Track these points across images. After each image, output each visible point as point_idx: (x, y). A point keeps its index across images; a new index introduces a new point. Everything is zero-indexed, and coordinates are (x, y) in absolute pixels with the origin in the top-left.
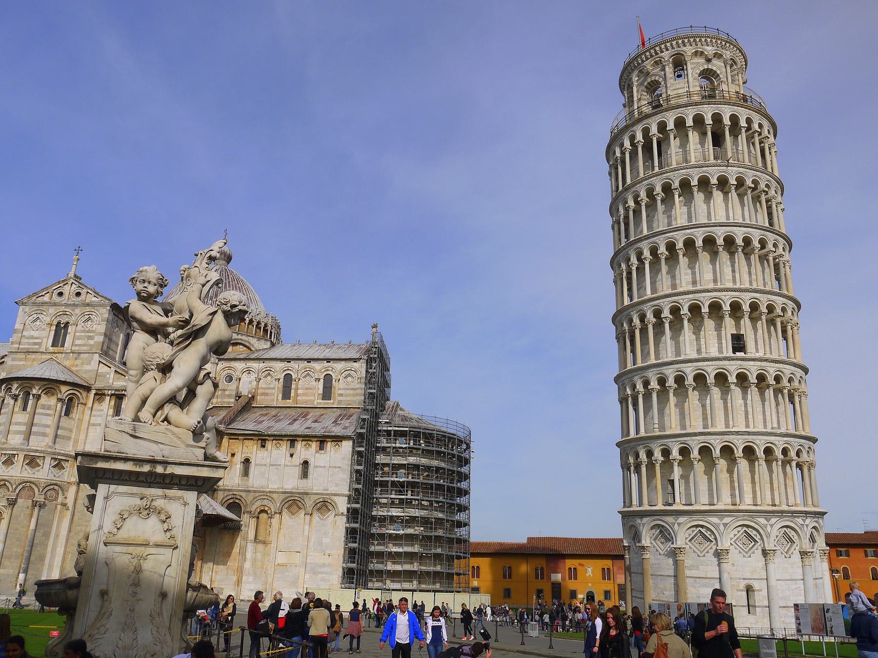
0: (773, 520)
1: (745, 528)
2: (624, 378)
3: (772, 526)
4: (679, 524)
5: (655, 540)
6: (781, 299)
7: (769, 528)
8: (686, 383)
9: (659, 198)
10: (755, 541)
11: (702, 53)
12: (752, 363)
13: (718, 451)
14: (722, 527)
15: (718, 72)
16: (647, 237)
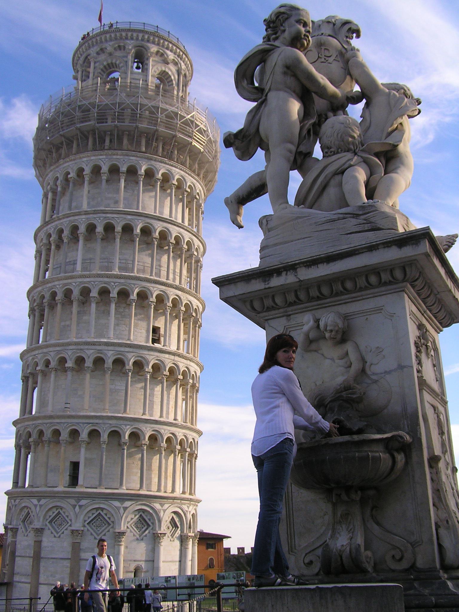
0: (166, 506)
1: (141, 513)
2: (37, 352)
3: (165, 511)
4: (80, 506)
5: (50, 522)
6: (196, 301)
7: (162, 512)
8: (106, 366)
9: (104, 177)
10: (149, 525)
11: (162, 55)
12: (167, 356)
13: (127, 437)
14: (122, 510)
15: (173, 78)
16: (86, 213)
